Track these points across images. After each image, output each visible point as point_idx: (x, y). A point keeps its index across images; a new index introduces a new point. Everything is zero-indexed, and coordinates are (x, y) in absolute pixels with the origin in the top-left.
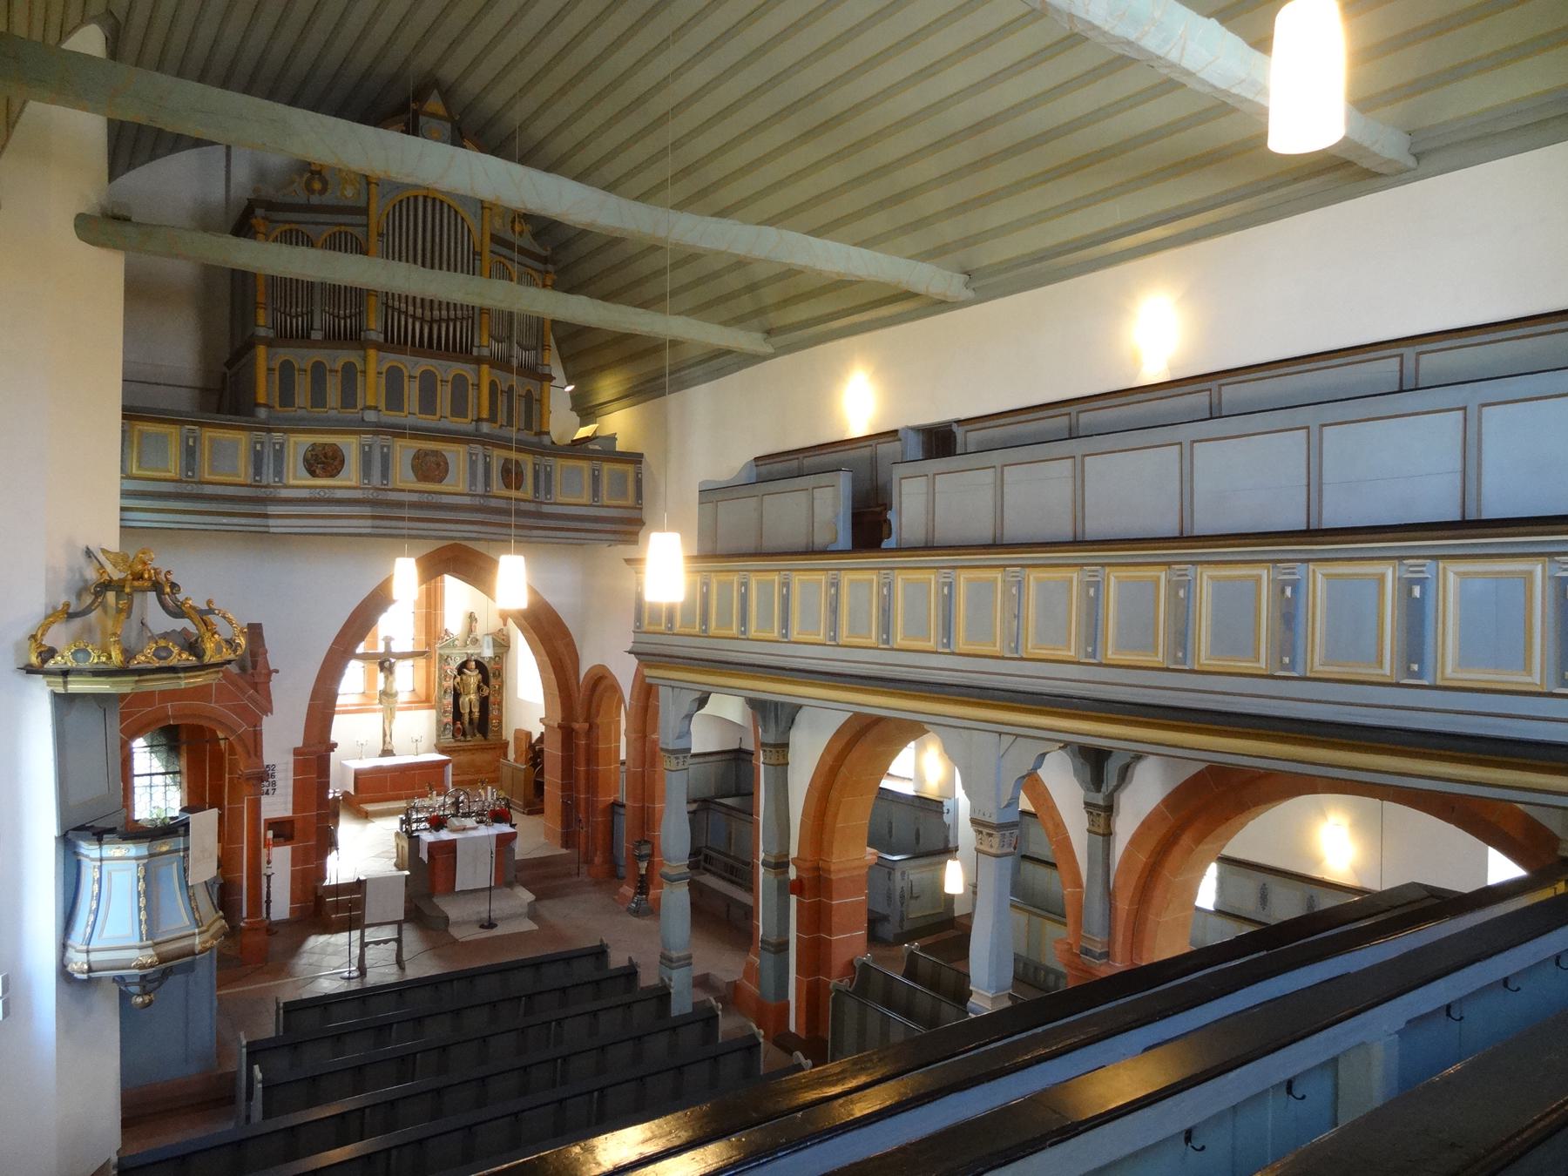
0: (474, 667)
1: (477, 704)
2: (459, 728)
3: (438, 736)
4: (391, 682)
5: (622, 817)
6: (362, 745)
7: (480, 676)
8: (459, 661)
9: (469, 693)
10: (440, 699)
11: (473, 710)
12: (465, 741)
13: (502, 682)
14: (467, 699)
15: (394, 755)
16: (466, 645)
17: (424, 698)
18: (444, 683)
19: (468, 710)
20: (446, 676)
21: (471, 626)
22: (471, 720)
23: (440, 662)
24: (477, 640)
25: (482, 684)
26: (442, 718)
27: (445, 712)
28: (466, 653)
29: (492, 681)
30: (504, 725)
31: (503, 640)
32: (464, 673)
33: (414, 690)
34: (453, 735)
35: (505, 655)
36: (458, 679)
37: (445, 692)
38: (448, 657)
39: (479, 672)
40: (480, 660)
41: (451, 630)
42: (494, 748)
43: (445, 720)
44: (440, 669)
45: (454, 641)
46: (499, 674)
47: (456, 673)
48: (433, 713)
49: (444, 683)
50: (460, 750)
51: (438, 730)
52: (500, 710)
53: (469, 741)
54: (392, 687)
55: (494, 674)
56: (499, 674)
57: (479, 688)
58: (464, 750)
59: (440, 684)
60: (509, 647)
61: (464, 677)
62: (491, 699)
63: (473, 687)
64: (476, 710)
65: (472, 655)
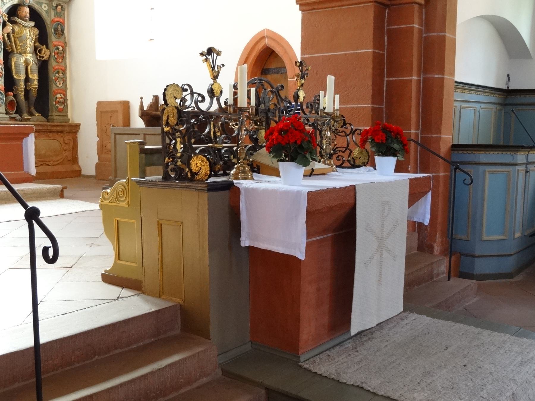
0: (28, 15)
1: (36, 69)
2: (12, 101)
5: (481, 168)
7: (36, 31)
9: (25, 52)
11: (30, 76)
14: (22, 60)
19: (23, 77)
22: (27, 92)
25: (37, 44)
29: (53, 39)
39: (34, 26)
40: (36, 6)
42: (61, 132)
46: (62, 31)
47: (6, 19)
53: (28, 120)
55: (56, 30)
56: (60, 32)
57: (35, 48)
62: (53, 64)
63: (30, 43)
64: (34, 77)
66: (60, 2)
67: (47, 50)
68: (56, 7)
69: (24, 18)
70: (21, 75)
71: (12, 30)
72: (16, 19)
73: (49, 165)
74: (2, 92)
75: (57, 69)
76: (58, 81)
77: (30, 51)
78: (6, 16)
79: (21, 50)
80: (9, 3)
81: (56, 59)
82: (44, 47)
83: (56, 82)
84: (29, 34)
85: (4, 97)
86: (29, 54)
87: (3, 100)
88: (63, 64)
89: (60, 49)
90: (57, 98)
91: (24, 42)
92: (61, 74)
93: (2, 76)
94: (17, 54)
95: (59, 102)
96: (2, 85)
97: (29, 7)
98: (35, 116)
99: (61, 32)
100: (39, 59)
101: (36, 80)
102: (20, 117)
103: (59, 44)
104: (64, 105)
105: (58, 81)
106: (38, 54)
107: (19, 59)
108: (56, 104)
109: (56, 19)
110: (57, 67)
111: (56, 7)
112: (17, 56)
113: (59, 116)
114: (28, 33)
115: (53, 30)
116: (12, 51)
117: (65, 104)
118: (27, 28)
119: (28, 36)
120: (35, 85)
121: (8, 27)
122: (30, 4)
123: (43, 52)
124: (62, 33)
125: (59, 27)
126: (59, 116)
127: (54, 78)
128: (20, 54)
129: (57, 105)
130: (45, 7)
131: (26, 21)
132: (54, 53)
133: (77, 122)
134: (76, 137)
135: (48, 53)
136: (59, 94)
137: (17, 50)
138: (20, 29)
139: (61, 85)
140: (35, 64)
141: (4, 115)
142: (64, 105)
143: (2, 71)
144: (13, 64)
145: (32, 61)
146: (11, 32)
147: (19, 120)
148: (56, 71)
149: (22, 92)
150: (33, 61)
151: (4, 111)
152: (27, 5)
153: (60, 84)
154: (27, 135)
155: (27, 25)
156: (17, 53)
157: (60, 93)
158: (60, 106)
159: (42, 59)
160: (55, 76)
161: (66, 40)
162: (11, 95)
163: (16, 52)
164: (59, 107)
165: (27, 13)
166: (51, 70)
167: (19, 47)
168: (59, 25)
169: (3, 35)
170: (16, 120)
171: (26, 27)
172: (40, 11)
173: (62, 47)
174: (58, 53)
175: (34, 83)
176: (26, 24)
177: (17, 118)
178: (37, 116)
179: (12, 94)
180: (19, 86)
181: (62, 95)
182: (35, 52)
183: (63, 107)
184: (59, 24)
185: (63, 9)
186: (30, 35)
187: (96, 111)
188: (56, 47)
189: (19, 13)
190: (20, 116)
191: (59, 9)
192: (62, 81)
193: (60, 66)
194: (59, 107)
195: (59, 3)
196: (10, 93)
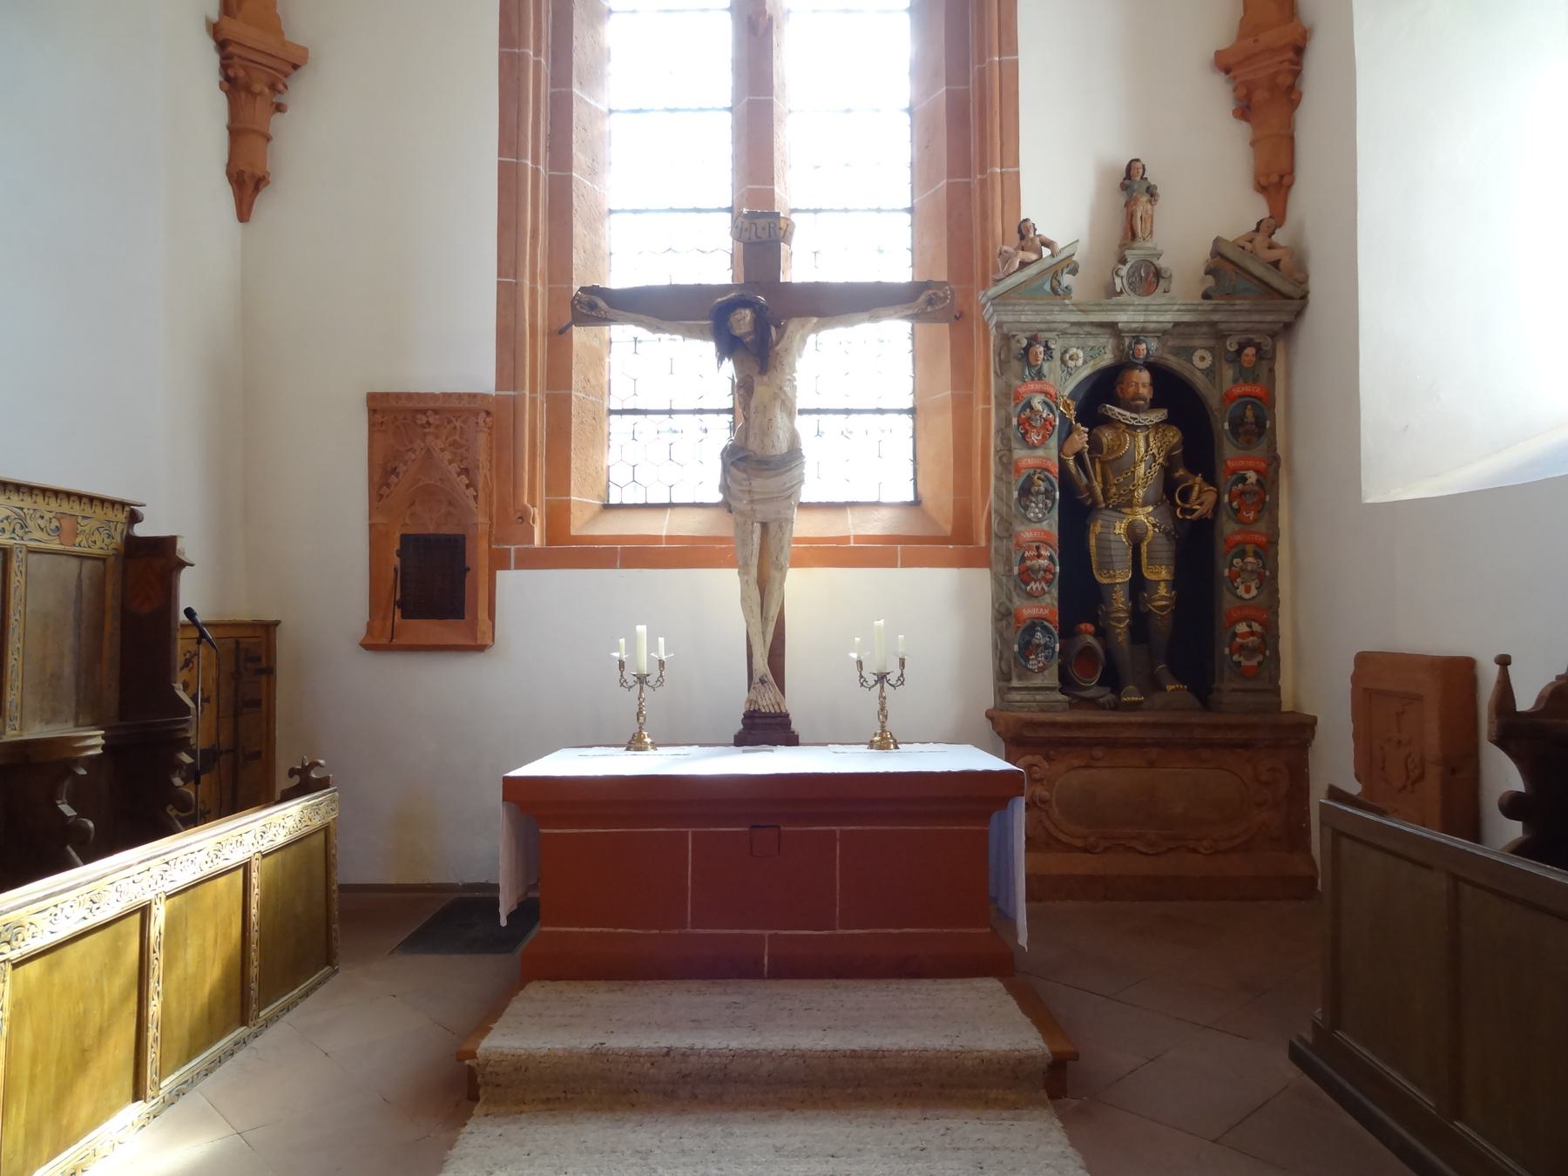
0: (1146, 392)
1: (1165, 549)
2: (1088, 651)
3: (1003, 676)
4: (765, 409)
6: (641, 679)
7: (1174, 436)
8: (1084, 370)
9: (1130, 504)
10: (1006, 523)
12: (1116, 707)
13: (1274, 460)
14: (1120, 528)
15: (791, 740)
16: (1112, 292)
17: (948, 529)
18: (1020, 453)
19: (1123, 576)
20: (1026, 425)
21: (1131, 217)
22: (1140, 620)
23: (1003, 365)
24: (1159, 274)
25: (1181, 472)
26: (1017, 602)
27: (1027, 575)
28: (1112, 327)
29: (1230, 453)
30: (1285, 646)
31: (1276, 264)
32: (1108, 421)
33: (917, 503)
34: (1064, 676)
35: (1280, 346)
36: (1080, 439)
37: (1026, 491)
38: (1033, 341)
40: (1173, 362)
41: (1044, 229)
42: (1246, 745)
43: (1030, 610)
44: (1008, 396)
45: (1055, 272)
47: (1071, 414)
48: (981, 580)
49: (1020, 453)
50: (1092, 744)
51: (1000, 652)
52: (1268, 581)
54: (767, 429)
55: (1237, 423)
58: (1112, 744)
59: (1007, 464)
60: (1304, 297)
61: (1107, 436)
64: (1160, 573)
65: (1139, 335)
66: (1251, 336)
67: (1206, 489)
68: (1236, 351)
69: (1132, 402)
70: (1114, 571)
71: (1088, 443)
72: (1106, 411)
73: (1199, 853)
74: (1050, 626)
75: (1237, 544)
76: (1242, 583)
77: (1144, 497)
78: (1067, 406)
79: (1118, 499)
80: (1084, 366)
81: (1237, 511)
82: (1199, 479)
83: (1236, 585)
84: (1142, 449)
85: (1055, 642)
86: (1144, 505)
87: (1054, 648)
88: (1262, 526)
89: (1248, 482)
90: (1235, 635)
91: (1126, 474)
92: (1250, 559)
93: (1053, 580)
94: (1107, 512)
95: (1242, 648)
96: (1053, 605)
97: (1152, 367)
98: (1166, 690)
99: (1254, 427)
100: (1180, 517)
101: (1162, 583)
102: (1110, 697)
103: (1250, 463)
104: (1260, 658)
105: (1242, 583)
106: (1178, 501)
107: (1109, 526)
108: (1232, 654)
109: (1238, 391)
110: (1239, 538)
111: (1240, 351)
112: (1105, 517)
113: (1245, 691)
114: (1142, 443)
115: (1226, 426)
116: (1095, 503)
117: (1268, 653)
118: (1139, 431)
119: (1139, 453)
120: (1159, 600)
121: (1076, 437)
122: (1152, 359)
123: (1195, 494)
124: (1256, 431)
125: (1249, 413)
126: (1245, 691)
127: (1226, 572)
128: (1117, 508)
129: (1236, 658)
130: (1203, 359)
131: (1136, 410)
132: (1230, 496)
133: (1308, 711)
134: (1305, 763)
135: (1210, 498)
136: (1244, 624)
137: (1106, 499)
138: (1118, 436)
139: (1254, 592)
140: (1161, 535)
141: (1054, 693)
142: (1260, 658)
143: (1052, 564)
144: (1093, 542)
145: (1150, 528)
146: (1086, 450)
147: (1108, 707)
148: (1234, 551)
149: (1120, 620)
150: (1154, 526)
151: (1055, 682)
152: (1142, 362)
153: (1248, 590)
154: (1002, 802)
155: (1140, 422)
156: (1107, 507)
157: (1248, 619)
158: (1248, 660)
159: (1188, 517)
160: (1232, 565)
161: (1280, 451)
162: (1087, 632)
163: (1103, 505)
164: (1245, 663)
165: (1140, 385)
166: (1221, 546)
167: (1114, 490)
168: (1249, 406)
169: (1062, 463)
170: (1102, 707)
171: (1138, 427)
172: (1187, 374)
173: (1257, 471)
174: (1242, 493)
175: (1158, 593)
176: (1135, 419)
177: (1101, 700)
178: (1173, 690)
179: (1090, 628)
180: (1112, 605)
181: (1253, 623)
182: (1168, 498)
183: (1260, 664)
184: (1247, 403)
185: (1265, 356)
186: (1146, 451)
187: (1350, 686)
188: (1235, 477)
189: (1118, 390)
190: (1112, 692)
191: (1247, 355)
192: (1257, 581)
193: (1253, 533)
194: (1242, 664)
195: (1251, 339)
196: (1083, 626)
